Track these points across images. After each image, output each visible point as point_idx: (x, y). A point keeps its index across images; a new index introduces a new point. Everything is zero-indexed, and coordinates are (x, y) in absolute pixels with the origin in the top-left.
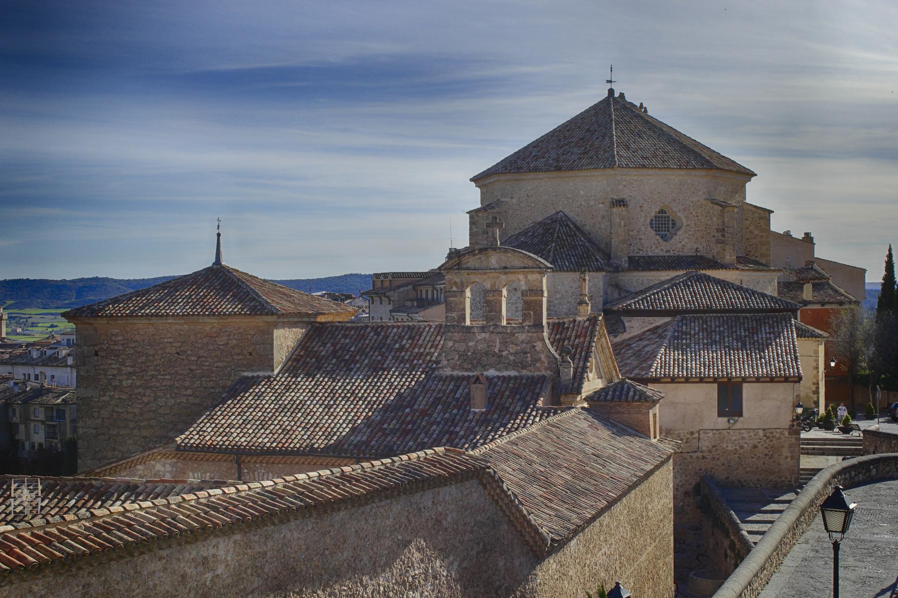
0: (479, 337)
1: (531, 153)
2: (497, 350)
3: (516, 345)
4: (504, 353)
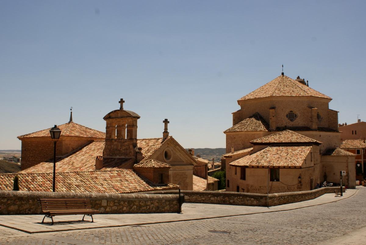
2: (119, 148)
3: (124, 146)
4: (121, 150)
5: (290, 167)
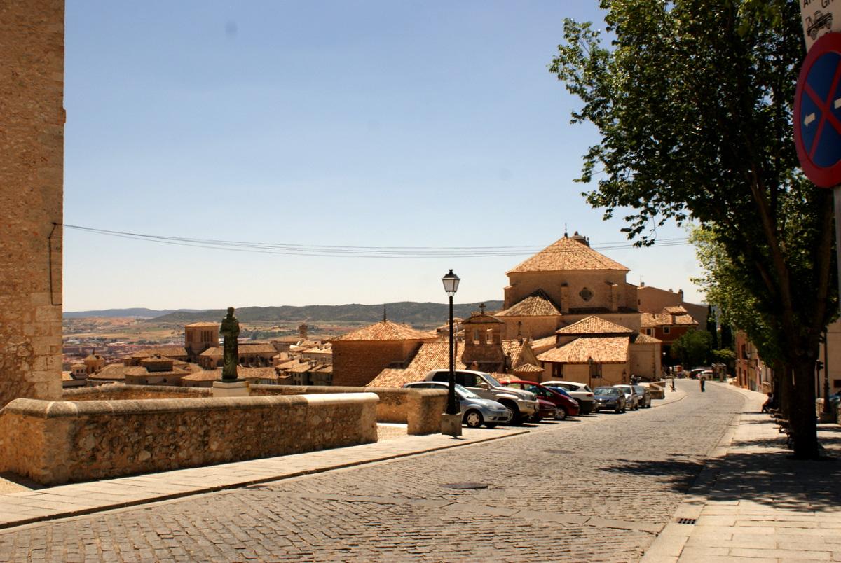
5: (613, 363)
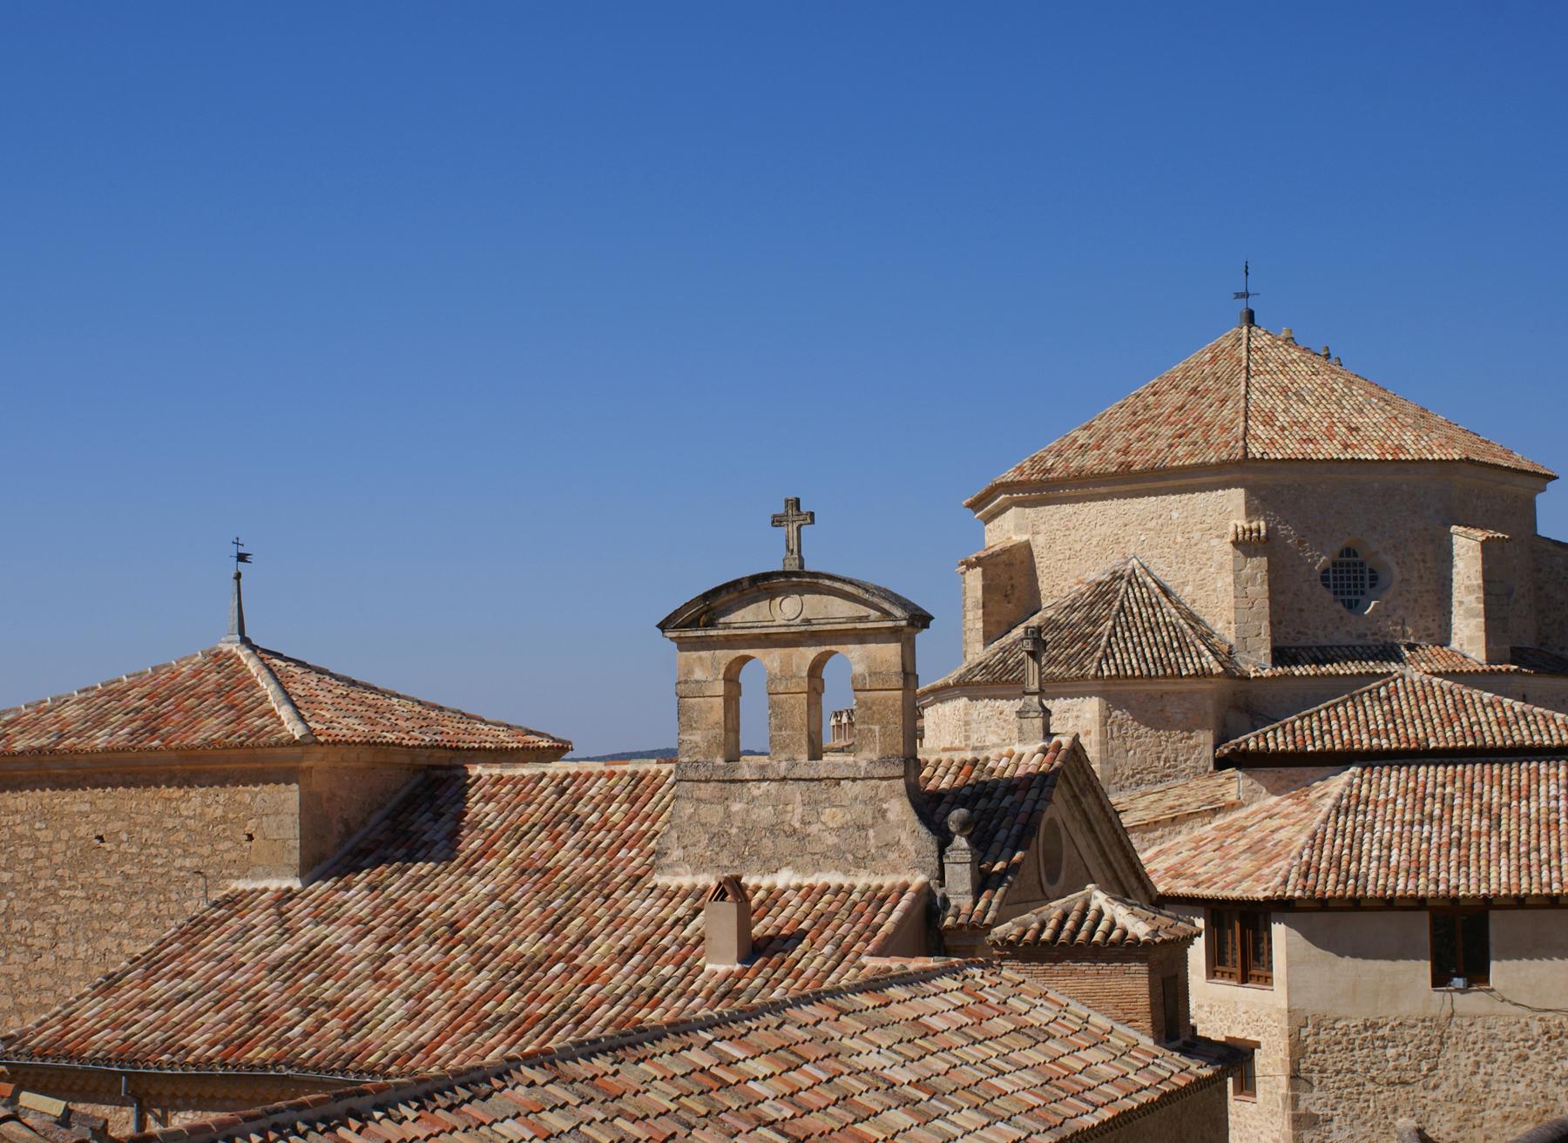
0: (756, 792)
1: (1075, 440)
